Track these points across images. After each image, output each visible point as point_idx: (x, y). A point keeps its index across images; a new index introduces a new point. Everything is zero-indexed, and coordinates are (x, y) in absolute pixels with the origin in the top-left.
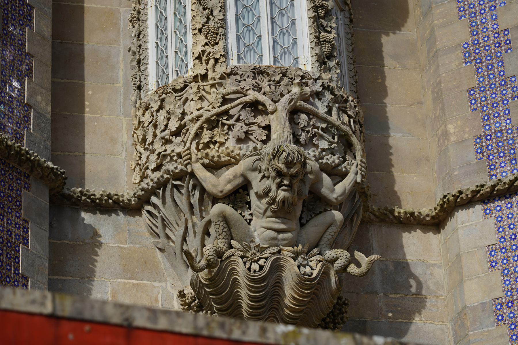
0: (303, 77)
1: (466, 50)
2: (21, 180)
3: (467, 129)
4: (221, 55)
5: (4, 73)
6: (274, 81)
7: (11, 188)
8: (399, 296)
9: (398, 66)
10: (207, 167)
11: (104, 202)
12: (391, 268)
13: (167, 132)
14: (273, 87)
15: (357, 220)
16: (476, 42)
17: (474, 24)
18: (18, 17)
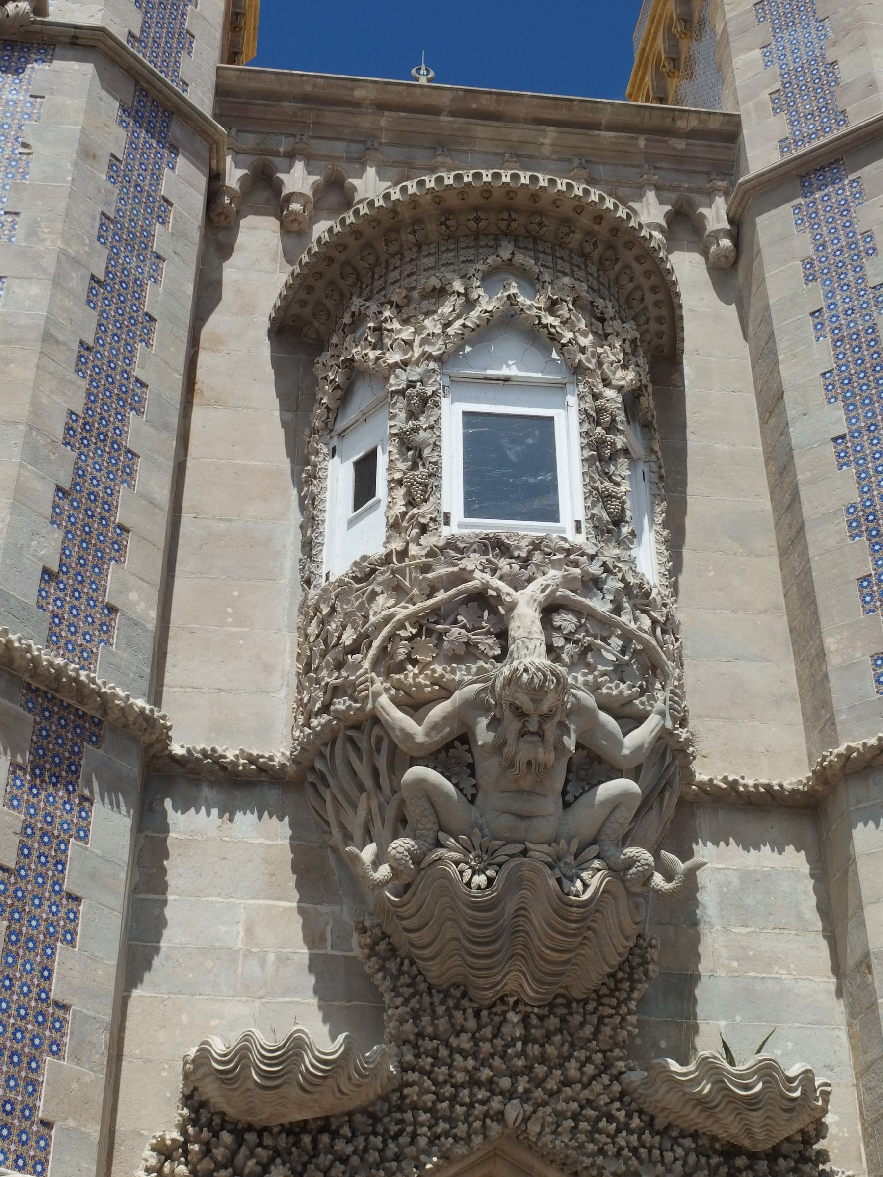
0: (568, 552)
1: (851, 517)
2: (83, 728)
3: (859, 644)
4: (431, 519)
5: (67, 552)
6: (519, 556)
7: (60, 741)
8: (748, 930)
9: (741, 550)
10: (399, 705)
11: (241, 768)
12: (736, 881)
13: (340, 648)
14: (516, 567)
15: (670, 799)
16: (868, 503)
17: (863, 475)
18: (107, 468)
